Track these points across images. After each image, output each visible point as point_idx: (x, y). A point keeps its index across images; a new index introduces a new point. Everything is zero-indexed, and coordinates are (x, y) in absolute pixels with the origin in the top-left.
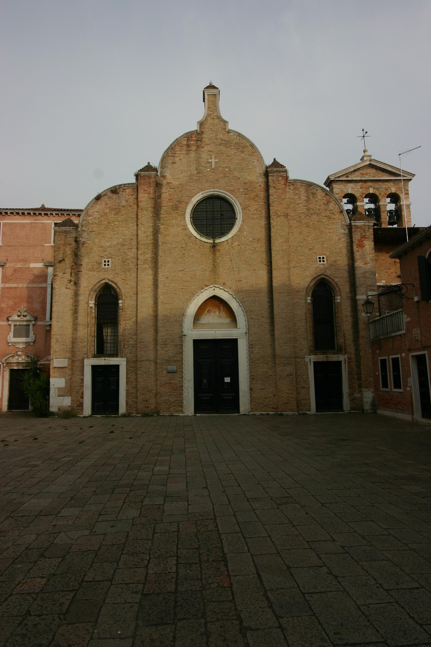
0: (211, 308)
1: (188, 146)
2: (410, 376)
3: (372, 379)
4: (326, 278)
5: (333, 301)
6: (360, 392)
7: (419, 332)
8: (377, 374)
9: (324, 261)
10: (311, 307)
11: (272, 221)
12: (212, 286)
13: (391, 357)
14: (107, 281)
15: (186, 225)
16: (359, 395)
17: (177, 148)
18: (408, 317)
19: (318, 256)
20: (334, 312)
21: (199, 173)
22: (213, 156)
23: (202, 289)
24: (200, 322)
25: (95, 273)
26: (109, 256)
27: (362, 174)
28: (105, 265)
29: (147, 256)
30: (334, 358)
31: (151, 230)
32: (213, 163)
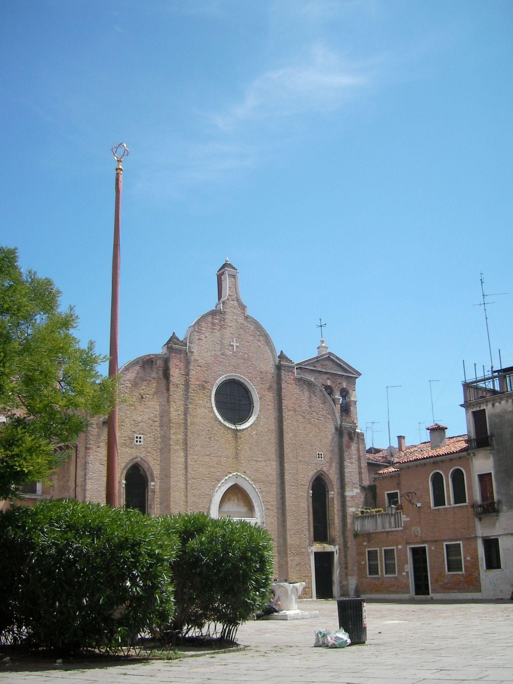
0: (230, 495)
1: (213, 324)
2: (407, 563)
3: (356, 568)
4: (324, 473)
5: (327, 496)
6: (347, 580)
7: (419, 529)
8: (363, 563)
9: (321, 458)
10: (311, 500)
11: (284, 415)
12: (235, 474)
13: (383, 548)
14: (139, 459)
15: (212, 408)
16: (346, 583)
17: (203, 324)
18: (407, 517)
19: (318, 453)
20: (327, 505)
21: (222, 354)
22: (235, 339)
23: (226, 476)
24: (221, 510)
25: (127, 449)
26: (142, 432)
27: (322, 365)
28: (137, 441)
29: (179, 436)
30: (329, 548)
31: (182, 409)
32: (235, 347)
